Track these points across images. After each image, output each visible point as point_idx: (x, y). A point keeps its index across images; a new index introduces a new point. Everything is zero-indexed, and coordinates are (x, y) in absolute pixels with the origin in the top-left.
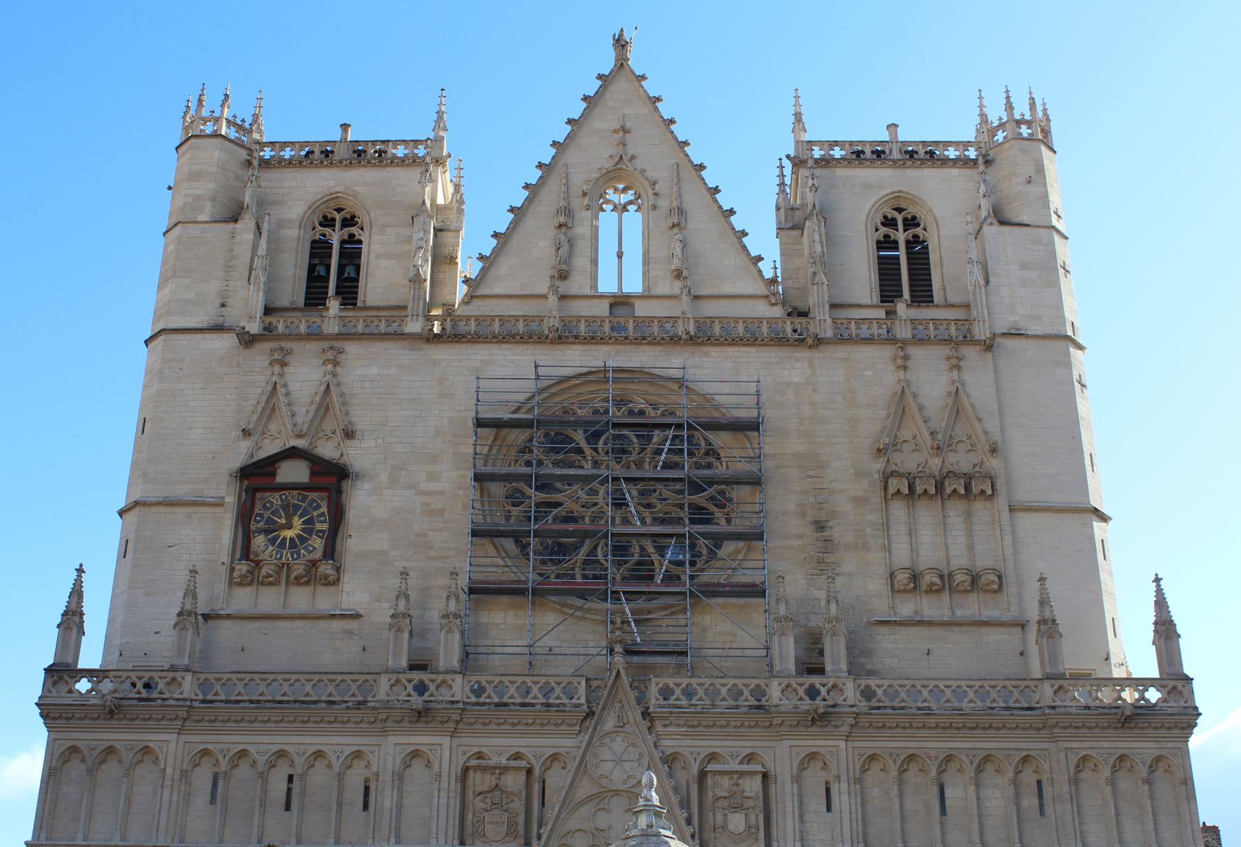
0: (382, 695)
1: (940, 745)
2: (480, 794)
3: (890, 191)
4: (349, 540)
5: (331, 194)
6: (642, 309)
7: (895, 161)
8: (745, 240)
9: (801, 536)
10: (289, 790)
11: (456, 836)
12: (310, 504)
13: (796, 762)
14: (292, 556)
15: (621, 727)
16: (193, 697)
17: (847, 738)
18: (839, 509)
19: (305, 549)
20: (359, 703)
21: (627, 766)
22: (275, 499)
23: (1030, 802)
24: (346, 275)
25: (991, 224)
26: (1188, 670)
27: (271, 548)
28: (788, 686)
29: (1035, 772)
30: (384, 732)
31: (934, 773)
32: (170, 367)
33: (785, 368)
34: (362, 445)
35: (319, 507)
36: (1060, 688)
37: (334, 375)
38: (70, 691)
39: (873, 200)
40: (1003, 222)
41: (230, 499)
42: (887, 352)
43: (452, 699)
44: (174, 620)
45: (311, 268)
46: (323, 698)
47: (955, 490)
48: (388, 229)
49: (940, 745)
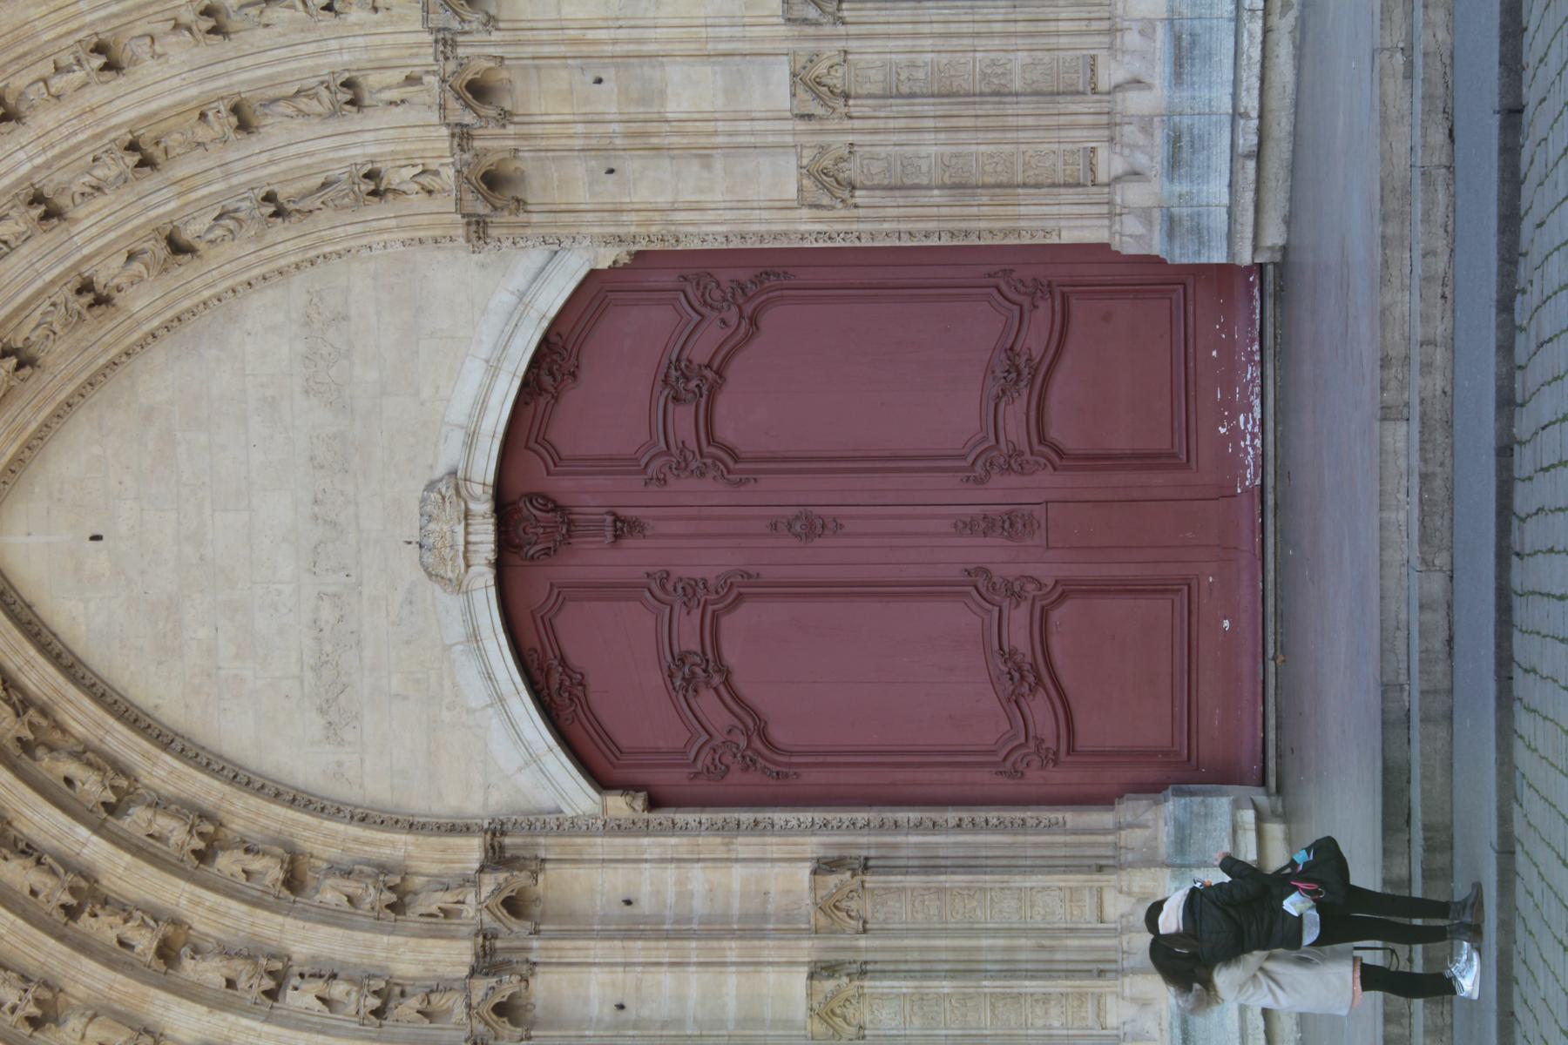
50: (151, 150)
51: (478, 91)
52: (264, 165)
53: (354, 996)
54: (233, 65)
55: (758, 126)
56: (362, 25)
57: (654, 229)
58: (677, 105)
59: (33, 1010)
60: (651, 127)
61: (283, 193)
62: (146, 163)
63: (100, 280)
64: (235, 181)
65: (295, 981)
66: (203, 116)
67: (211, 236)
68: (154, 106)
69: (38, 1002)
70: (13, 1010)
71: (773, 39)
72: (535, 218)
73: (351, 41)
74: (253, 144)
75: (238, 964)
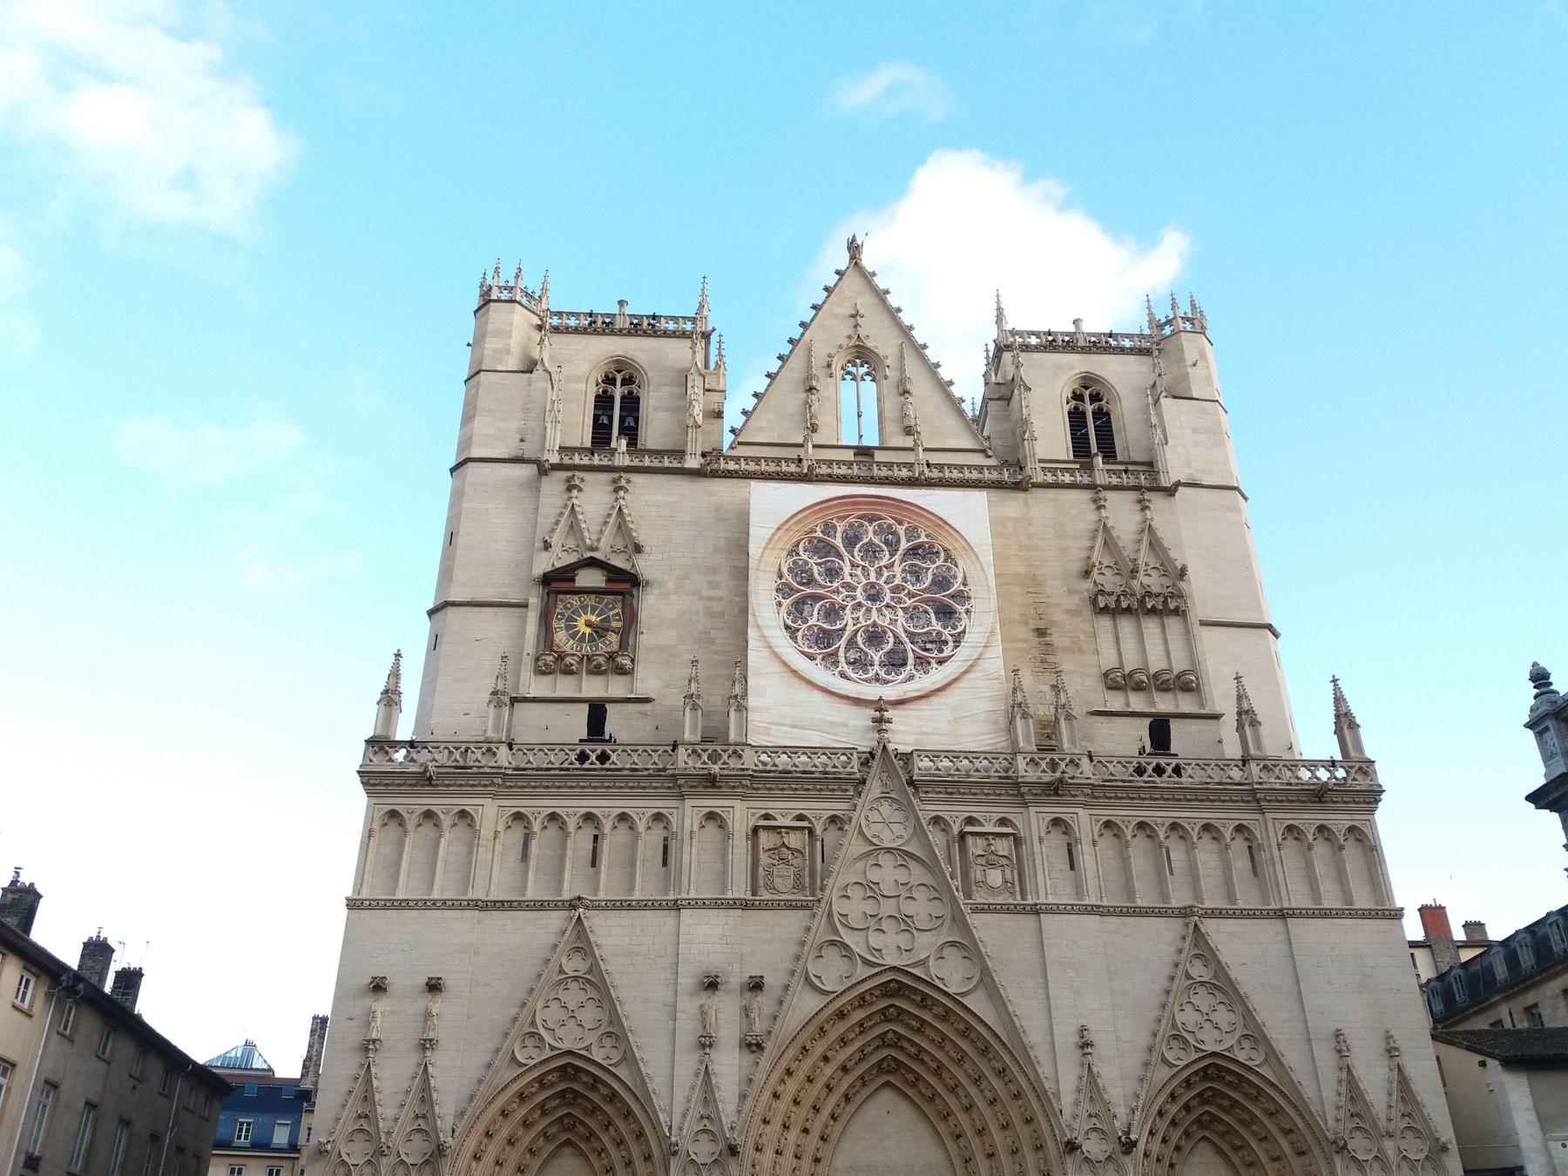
0: (681, 764)
1: (1164, 814)
2: (769, 850)
3: (1077, 371)
4: (641, 636)
5: (612, 357)
6: (880, 456)
7: (1082, 348)
8: (963, 405)
9: (1025, 640)
10: (595, 848)
11: (749, 888)
12: (606, 605)
13: (1043, 826)
14: (591, 649)
15: (888, 793)
16: (507, 765)
17: (1085, 805)
18: (1056, 619)
19: (601, 642)
20: (660, 770)
21: (894, 827)
22: (575, 601)
23: (1241, 864)
24: (627, 424)
25: (1166, 397)
26: (1369, 754)
27: (572, 642)
28: (1032, 760)
29: (1246, 839)
30: (682, 797)
31: (1162, 838)
32: (475, 490)
33: (1004, 506)
34: (651, 558)
35: (614, 608)
36: (1265, 767)
37: (624, 499)
38: (391, 760)
39: (1065, 378)
40: (1175, 397)
41: (534, 601)
42: (1086, 495)
43: (743, 767)
44: (487, 697)
45: (596, 418)
46: (628, 766)
47: (1153, 606)
48: (663, 388)
49: (1164, 814)
63: (950, 1118)
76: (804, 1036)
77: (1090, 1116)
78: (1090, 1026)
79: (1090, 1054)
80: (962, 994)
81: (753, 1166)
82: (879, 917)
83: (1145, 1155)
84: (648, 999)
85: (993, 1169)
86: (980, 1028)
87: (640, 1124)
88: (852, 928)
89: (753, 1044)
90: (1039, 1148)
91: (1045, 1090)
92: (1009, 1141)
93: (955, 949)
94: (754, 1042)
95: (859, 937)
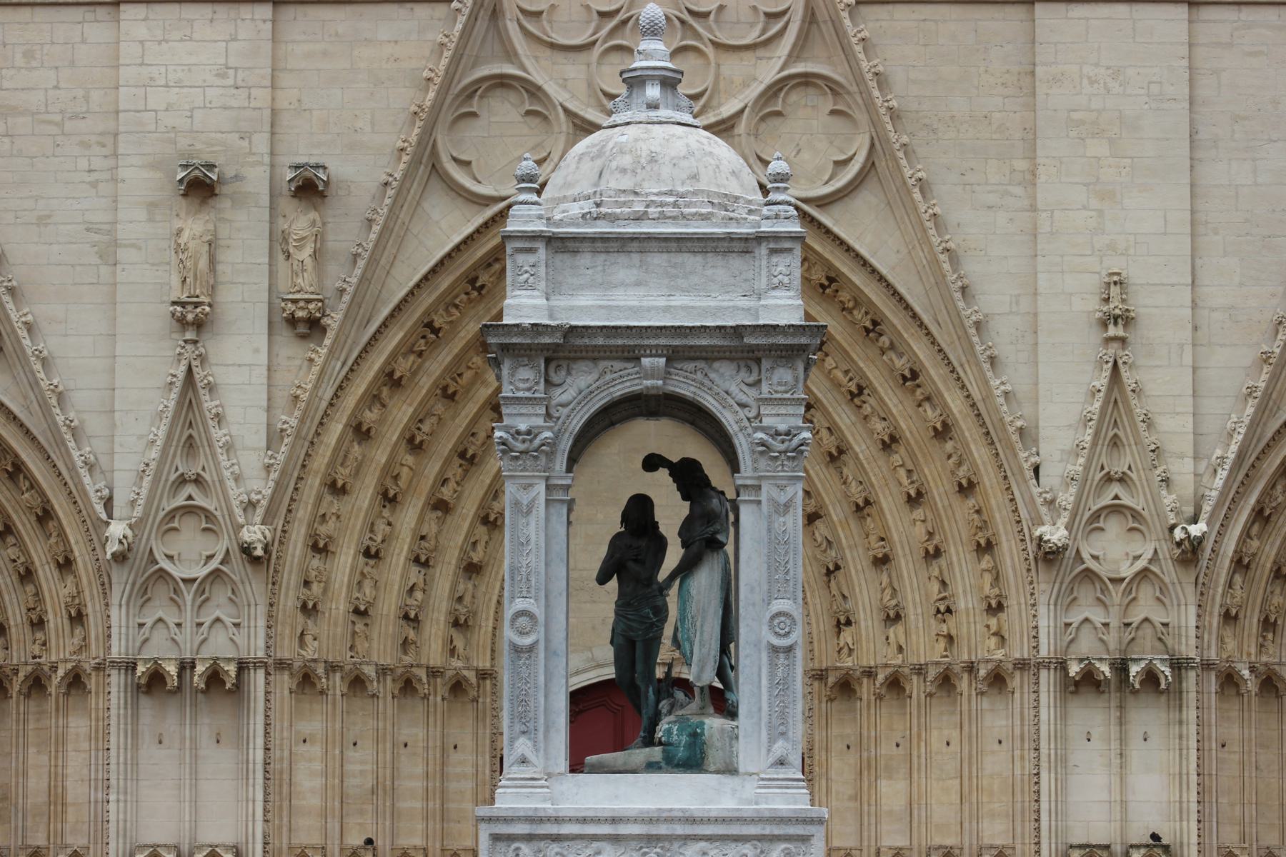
50: (865, 511)
51: (895, 684)
52: (855, 567)
53: (416, 603)
54: (910, 559)
55: (873, 827)
56: (929, 626)
57: (817, 769)
58: (884, 785)
59: (418, 439)
60: (873, 771)
61: (840, 574)
62: (859, 509)
64: (847, 552)
65: (423, 572)
66: (883, 539)
67: (817, 534)
68: (889, 517)
69: (421, 442)
70: (419, 429)
71: (919, 838)
72: (824, 705)
73: (921, 620)
74: (866, 563)
75: (433, 542)
76: (427, 299)
77: (1109, 479)
78: (1135, 274)
79: (1123, 341)
80: (823, 202)
81: (307, 583)
82: (622, 16)
83: (1241, 564)
84: (49, 216)
85: (883, 591)
86: (857, 278)
87: (42, 493)
88: (553, 46)
89: (301, 320)
90: (986, 548)
91: (1001, 419)
92: (920, 531)
93: (811, 91)
94: (300, 314)
95: (573, 69)
